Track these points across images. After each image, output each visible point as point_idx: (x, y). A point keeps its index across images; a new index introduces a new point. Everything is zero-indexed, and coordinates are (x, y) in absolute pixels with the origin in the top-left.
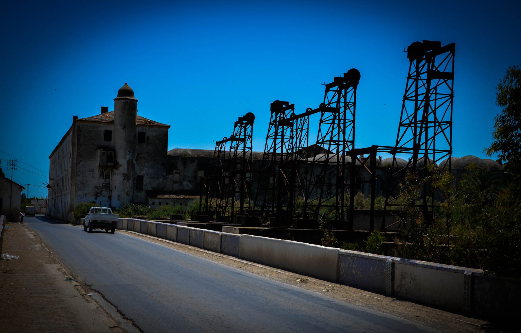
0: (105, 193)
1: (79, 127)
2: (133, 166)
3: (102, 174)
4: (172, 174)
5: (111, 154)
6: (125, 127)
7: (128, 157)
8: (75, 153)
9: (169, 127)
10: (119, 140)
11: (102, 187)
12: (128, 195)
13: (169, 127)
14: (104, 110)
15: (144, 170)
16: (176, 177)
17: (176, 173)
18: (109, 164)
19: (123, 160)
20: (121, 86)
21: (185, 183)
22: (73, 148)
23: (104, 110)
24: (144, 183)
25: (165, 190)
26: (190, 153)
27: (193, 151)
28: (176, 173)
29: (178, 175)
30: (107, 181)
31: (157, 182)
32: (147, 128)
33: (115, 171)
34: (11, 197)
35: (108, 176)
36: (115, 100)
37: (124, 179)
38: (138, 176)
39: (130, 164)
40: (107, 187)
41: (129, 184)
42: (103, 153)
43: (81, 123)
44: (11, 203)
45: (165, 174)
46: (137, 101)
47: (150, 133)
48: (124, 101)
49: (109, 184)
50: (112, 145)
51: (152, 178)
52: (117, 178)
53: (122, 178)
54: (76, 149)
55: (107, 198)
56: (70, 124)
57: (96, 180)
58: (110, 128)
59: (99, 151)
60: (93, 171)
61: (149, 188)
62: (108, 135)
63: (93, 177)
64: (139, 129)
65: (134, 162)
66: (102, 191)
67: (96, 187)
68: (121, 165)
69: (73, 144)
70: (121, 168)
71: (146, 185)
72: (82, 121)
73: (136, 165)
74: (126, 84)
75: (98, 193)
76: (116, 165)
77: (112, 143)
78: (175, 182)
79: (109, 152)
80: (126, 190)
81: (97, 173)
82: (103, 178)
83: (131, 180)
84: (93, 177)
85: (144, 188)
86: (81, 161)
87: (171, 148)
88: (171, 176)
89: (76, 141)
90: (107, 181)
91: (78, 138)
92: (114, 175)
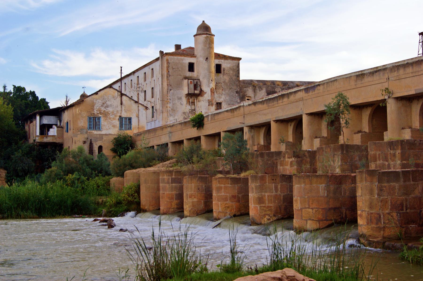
3: (188, 102)
5: (196, 82)
6: (207, 58)
8: (165, 84)
10: (203, 72)
13: (240, 59)
14: (178, 47)
17: (247, 99)
22: (162, 78)
23: (178, 47)
28: (247, 99)
30: (193, 107)
32: (223, 61)
33: (200, 98)
34: (138, 116)
35: (193, 103)
36: (194, 36)
38: (217, 103)
39: (212, 91)
42: (191, 82)
43: (170, 57)
44: (139, 122)
45: (239, 101)
47: (225, 65)
48: (205, 36)
49: (195, 110)
50: (195, 76)
51: (229, 104)
53: (207, 104)
58: (192, 60)
60: (180, 99)
62: (191, 67)
64: (217, 62)
67: (184, 113)
68: (206, 93)
69: (162, 76)
70: (206, 95)
72: (167, 54)
73: (215, 93)
74: (203, 21)
76: (201, 93)
77: (194, 74)
81: (184, 100)
83: (214, 106)
84: (181, 104)
86: (171, 90)
87: (241, 78)
90: (193, 107)
91: (167, 69)
92: (199, 101)
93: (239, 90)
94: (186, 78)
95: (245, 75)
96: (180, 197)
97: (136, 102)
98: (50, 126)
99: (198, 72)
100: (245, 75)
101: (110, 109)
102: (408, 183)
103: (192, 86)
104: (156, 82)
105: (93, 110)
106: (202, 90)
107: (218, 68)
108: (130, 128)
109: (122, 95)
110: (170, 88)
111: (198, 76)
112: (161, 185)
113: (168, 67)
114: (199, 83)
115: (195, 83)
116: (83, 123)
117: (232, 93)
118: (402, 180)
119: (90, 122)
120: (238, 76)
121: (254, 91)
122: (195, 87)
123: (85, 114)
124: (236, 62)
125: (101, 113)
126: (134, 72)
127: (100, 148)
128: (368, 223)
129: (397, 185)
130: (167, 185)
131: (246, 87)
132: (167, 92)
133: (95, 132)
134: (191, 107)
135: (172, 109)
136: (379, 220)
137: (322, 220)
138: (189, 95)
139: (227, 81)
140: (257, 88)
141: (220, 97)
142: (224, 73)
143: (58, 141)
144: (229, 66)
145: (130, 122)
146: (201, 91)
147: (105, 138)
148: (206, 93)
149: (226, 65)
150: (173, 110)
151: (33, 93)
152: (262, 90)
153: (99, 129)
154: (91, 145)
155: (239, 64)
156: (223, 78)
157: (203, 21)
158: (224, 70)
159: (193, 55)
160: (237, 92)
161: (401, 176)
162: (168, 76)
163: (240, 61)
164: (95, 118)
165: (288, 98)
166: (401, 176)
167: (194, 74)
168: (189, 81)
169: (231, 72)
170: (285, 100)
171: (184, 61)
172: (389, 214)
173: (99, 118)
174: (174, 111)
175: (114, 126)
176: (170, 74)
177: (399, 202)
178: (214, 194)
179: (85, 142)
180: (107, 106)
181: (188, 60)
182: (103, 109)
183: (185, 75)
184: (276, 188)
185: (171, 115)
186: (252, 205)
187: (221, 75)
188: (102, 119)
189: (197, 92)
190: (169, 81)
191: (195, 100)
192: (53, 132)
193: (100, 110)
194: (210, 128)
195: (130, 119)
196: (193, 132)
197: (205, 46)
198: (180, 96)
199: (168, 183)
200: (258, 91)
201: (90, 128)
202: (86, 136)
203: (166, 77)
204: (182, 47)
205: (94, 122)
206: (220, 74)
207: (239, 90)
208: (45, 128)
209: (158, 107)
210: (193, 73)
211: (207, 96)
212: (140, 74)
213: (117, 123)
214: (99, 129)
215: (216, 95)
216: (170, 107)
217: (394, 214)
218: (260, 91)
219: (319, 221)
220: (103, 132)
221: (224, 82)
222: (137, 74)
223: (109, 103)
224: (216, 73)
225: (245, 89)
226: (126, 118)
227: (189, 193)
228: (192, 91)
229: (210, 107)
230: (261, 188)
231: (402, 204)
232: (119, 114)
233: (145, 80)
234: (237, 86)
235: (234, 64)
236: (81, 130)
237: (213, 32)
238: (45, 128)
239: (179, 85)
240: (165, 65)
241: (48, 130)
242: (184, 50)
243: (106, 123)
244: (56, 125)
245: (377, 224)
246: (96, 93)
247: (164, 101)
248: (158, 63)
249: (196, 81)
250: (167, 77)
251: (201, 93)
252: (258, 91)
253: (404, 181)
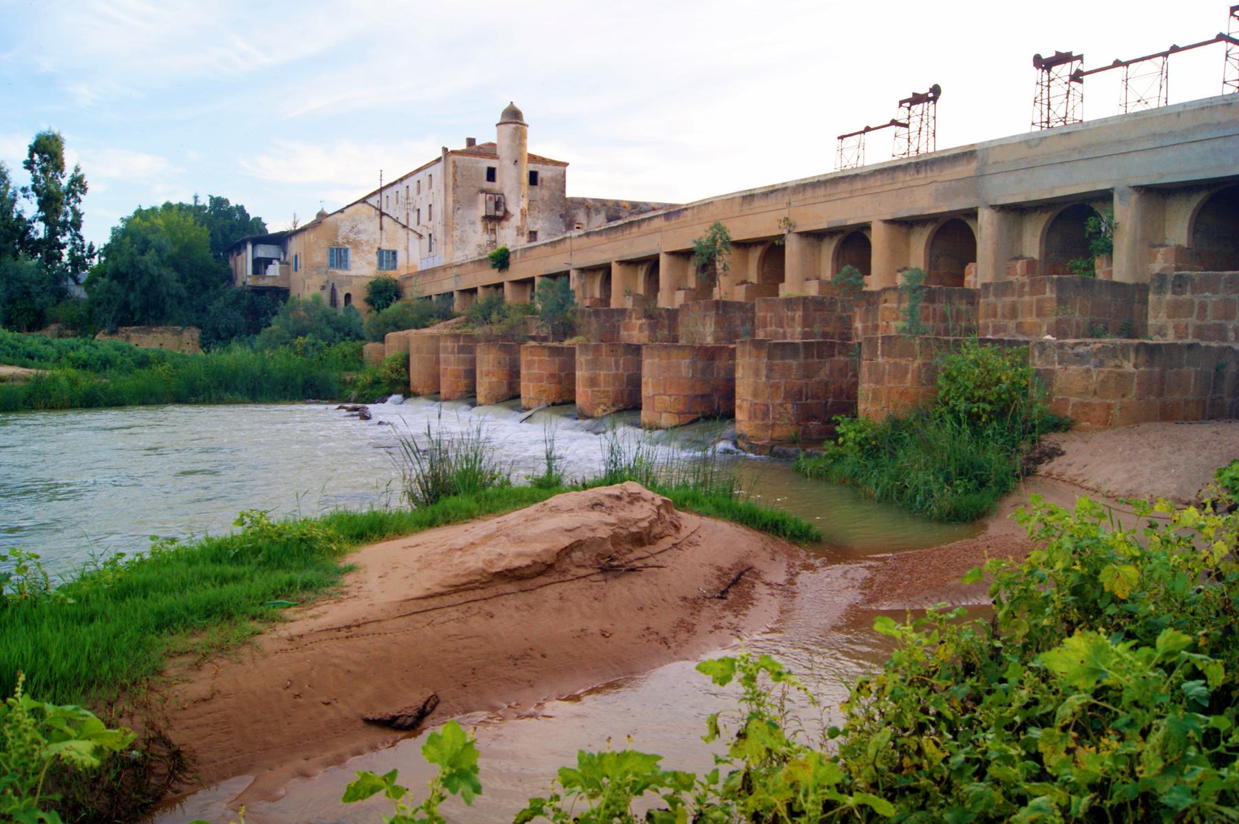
1: (454, 162)
3: (486, 228)
8: (450, 199)
9: (566, 164)
10: (510, 182)
14: (471, 142)
15: (539, 224)
19: (516, 205)
20: (507, 105)
22: (446, 190)
23: (471, 142)
27: (594, 200)
33: (504, 223)
35: (493, 230)
47: (544, 173)
59: (482, 196)
60: (473, 223)
62: (491, 174)
64: (532, 167)
67: (479, 246)
69: (446, 186)
72: (453, 152)
76: (506, 216)
77: (496, 186)
81: (480, 226)
87: (569, 194)
95: (574, 190)
96: (471, 374)
97: (404, 227)
98: (268, 261)
100: (574, 190)
101: (363, 237)
102: (810, 360)
103: (492, 204)
104: (436, 196)
105: (336, 236)
107: (533, 178)
108: (395, 267)
109: (382, 214)
112: (442, 355)
113: (455, 174)
116: (321, 256)
118: (802, 355)
119: (332, 255)
120: (564, 192)
121: (588, 215)
122: (497, 205)
123: (324, 243)
124: (561, 168)
125: (348, 243)
126: (401, 180)
127: (348, 297)
128: (750, 419)
129: (794, 363)
130: (452, 357)
133: (340, 272)
136: (766, 414)
137: (683, 413)
138: (488, 218)
139: (546, 198)
141: (535, 223)
143: (281, 284)
145: (395, 258)
146: (506, 212)
147: (355, 282)
150: (462, 241)
151: (241, 209)
153: (346, 267)
154: (333, 291)
156: (541, 192)
159: (494, 156)
160: (561, 216)
161: (801, 349)
162: (455, 186)
164: (339, 250)
165: (639, 227)
166: (801, 349)
167: (496, 186)
170: (635, 229)
172: (781, 405)
173: (346, 251)
175: (369, 263)
177: (796, 389)
178: (523, 371)
179: (323, 288)
180: (359, 232)
181: (487, 163)
182: (352, 236)
184: (617, 363)
185: (458, 249)
186: (580, 389)
187: (537, 189)
188: (350, 252)
189: (499, 213)
192: (274, 270)
193: (346, 238)
194: (519, 270)
195: (394, 253)
196: (493, 276)
199: (453, 352)
201: (332, 266)
202: (325, 278)
203: (450, 190)
204: (478, 143)
205: (339, 256)
208: (260, 265)
209: (439, 235)
211: (515, 220)
212: (412, 182)
213: (375, 259)
214: (346, 267)
215: (529, 220)
217: (789, 406)
219: (679, 413)
220: (353, 273)
221: (542, 199)
222: (406, 183)
223: (361, 227)
226: (388, 251)
227: (485, 369)
228: (491, 212)
230: (594, 364)
231: (800, 391)
232: (377, 245)
233: (419, 193)
234: (562, 206)
236: (317, 268)
237: (526, 120)
238: (260, 265)
239: (472, 202)
240: (451, 169)
241: (266, 268)
242: (480, 147)
243: (356, 259)
244: (279, 259)
245: (763, 419)
246: (342, 211)
247: (448, 226)
248: (440, 166)
251: (506, 216)
253: (806, 358)
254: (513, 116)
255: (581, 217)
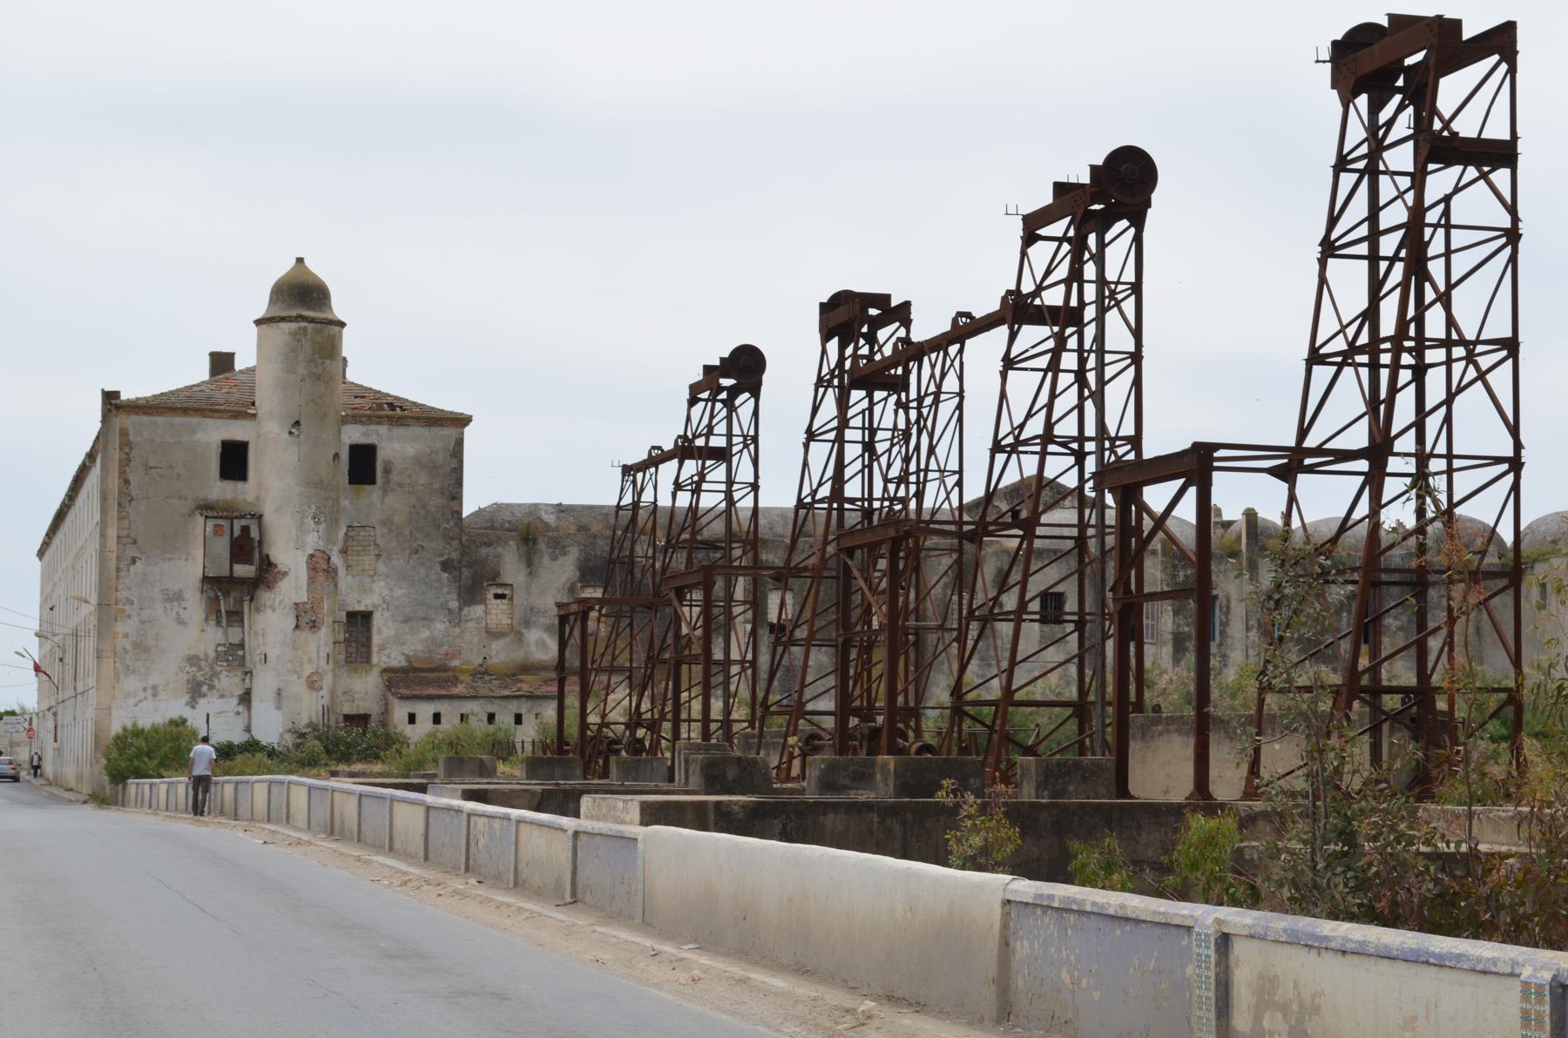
0: (229, 682)
1: (124, 433)
2: (331, 572)
4: (483, 601)
5: (246, 529)
6: (297, 423)
7: (312, 541)
8: (112, 533)
11: (217, 658)
12: (313, 685)
13: (464, 421)
14: (221, 363)
15: (374, 590)
16: (498, 612)
18: (242, 570)
19: (289, 551)
20: (284, 267)
21: (533, 635)
22: (104, 512)
23: (221, 363)
24: (376, 639)
25: (455, 663)
26: (550, 519)
27: (561, 509)
28: (497, 596)
29: (503, 605)
30: (234, 635)
31: (425, 634)
32: (383, 429)
33: (264, 596)
35: (236, 617)
36: (258, 322)
37: (297, 627)
38: (351, 615)
39: (320, 567)
40: (235, 655)
41: (321, 644)
43: (134, 418)
45: (454, 604)
46: (343, 325)
47: (394, 446)
48: (294, 326)
49: (241, 646)
50: (250, 498)
51: (407, 620)
52: (271, 623)
53: (292, 622)
54: (113, 513)
55: (235, 701)
56: (91, 421)
57: (194, 633)
58: (236, 431)
60: (178, 597)
61: (397, 661)
62: (234, 460)
63: (181, 622)
64: (355, 434)
65: (336, 559)
66: (215, 674)
67: (193, 660)
68: (285, 574)
71: (382, 648)
73: (342, 572)
74: (300, 260)
75: (200, 684)
76: (267, 573)
78: (494, 634)
79: (237, 525)
80: (308, 670)
81: (195, 605)
82: (219, 623)
83: (324, 633)
85: (375, 659)
86: (134, 561)
87: (471, 504)
88: (478, 610)
89: (114, 483)
90: (234, 635)
91: (122, 473)
93: (455, 555)
94: (207, 509)
99: (259, 485)
103: (222, 546)
106: (270, 564)
107: (363, 465)
110: (131, 552)
111: (258, 498)
113: (125, 463)
114: (254, 534)
115: (237, 532)
117: (423, 571)
120: (456, 497)
121: (529, 561)
124: (449, 432)
131: (488, 545)
132: (118, 570)
134: (226, 634)
135: (136, 645)
139: (398, 519)
140: (542, 546)
141: (364, 590)
142: (387, 482)
144: (411, 450)
146: (267, 565)
148: (285, 574)
149: (397, 446)
150: (141, 647)
152: (564, 553)
155: (460, 442)
157: (300, 260)
158: (387, 471)
160: (446, 566)
163: (467, 431)
168: (211, 523)
169: (423, 478)
171: (200, 436)
174: (147, 649)
176: (134, 492)
181: (216, 432)
183: (202, 496)
185: (130, 671)
187: (372, 494)
189: (242, 570)
190: (126, 522)
191: (246, 604)
197: (290, 370)
198: (174, 587)
200: (546, 559)
206: (367, 487)
207: (455, 555)
210: (240, 485)
211: (293, 586)
216: (126, 636)
218: (554, 558)
221: (387, 522)
224: (351, 482)
225: (484, 551)
229: (305, 635)
234: (448, 538)
235: (438, 444)
237: (339, 309)
239: (171, 542)
249: (244, 522)
250: (119, 505)
252: (546, 559)
254: (301, 300)
255: (512, 568)
